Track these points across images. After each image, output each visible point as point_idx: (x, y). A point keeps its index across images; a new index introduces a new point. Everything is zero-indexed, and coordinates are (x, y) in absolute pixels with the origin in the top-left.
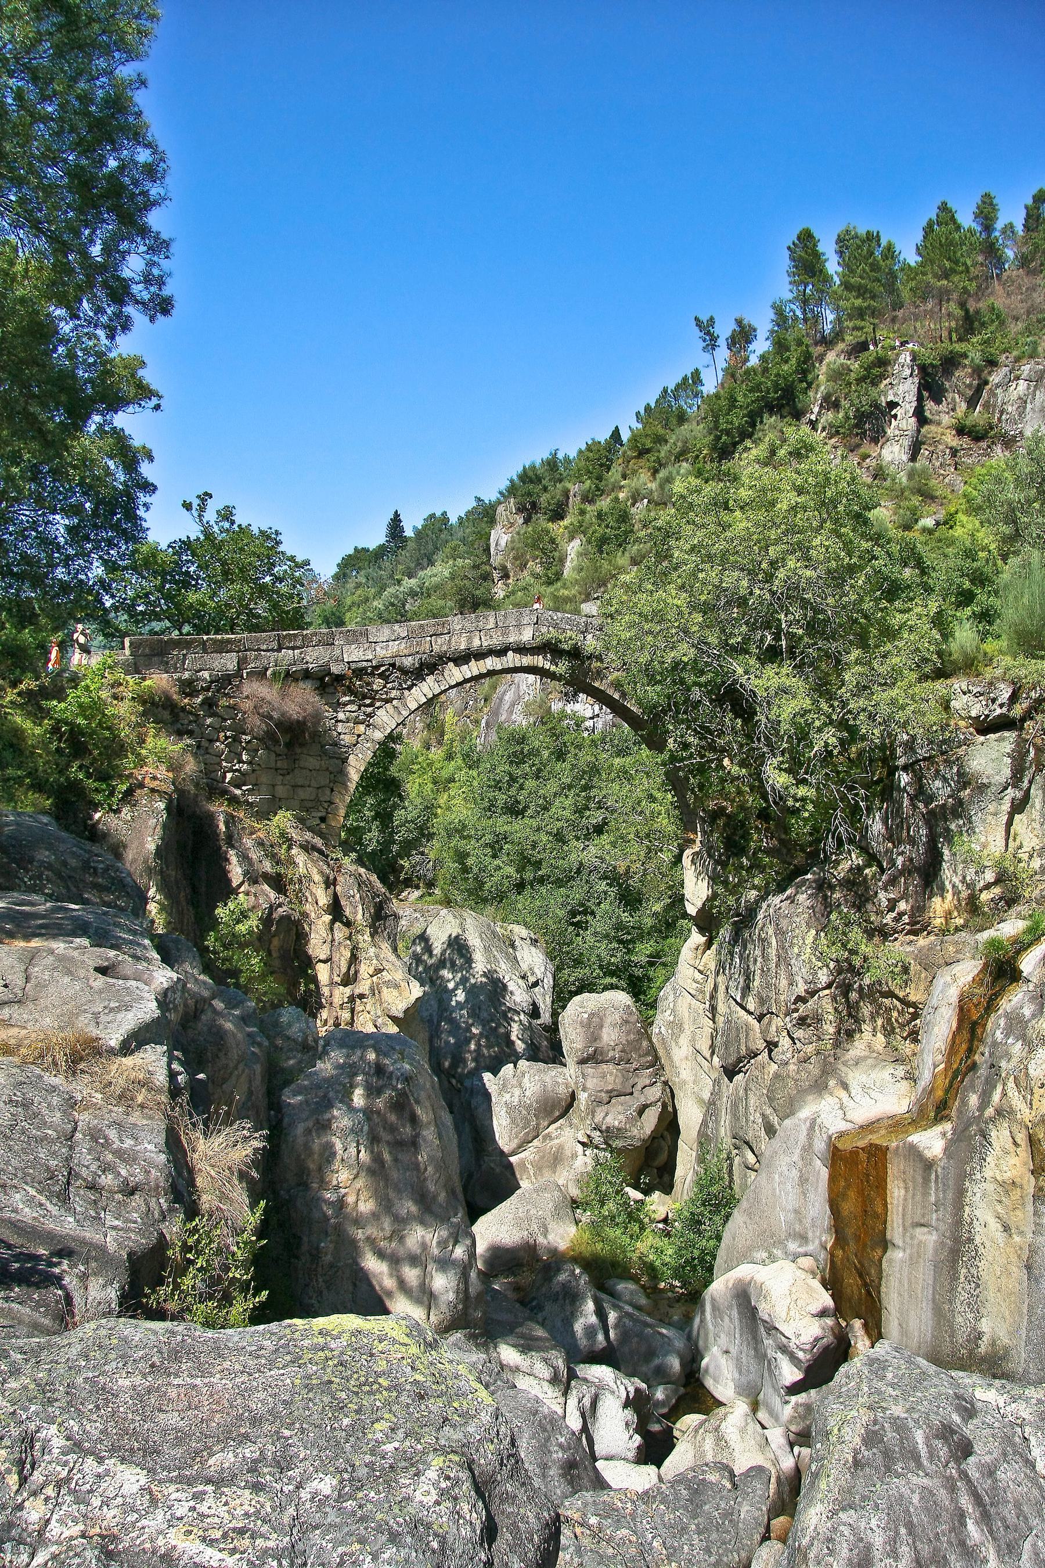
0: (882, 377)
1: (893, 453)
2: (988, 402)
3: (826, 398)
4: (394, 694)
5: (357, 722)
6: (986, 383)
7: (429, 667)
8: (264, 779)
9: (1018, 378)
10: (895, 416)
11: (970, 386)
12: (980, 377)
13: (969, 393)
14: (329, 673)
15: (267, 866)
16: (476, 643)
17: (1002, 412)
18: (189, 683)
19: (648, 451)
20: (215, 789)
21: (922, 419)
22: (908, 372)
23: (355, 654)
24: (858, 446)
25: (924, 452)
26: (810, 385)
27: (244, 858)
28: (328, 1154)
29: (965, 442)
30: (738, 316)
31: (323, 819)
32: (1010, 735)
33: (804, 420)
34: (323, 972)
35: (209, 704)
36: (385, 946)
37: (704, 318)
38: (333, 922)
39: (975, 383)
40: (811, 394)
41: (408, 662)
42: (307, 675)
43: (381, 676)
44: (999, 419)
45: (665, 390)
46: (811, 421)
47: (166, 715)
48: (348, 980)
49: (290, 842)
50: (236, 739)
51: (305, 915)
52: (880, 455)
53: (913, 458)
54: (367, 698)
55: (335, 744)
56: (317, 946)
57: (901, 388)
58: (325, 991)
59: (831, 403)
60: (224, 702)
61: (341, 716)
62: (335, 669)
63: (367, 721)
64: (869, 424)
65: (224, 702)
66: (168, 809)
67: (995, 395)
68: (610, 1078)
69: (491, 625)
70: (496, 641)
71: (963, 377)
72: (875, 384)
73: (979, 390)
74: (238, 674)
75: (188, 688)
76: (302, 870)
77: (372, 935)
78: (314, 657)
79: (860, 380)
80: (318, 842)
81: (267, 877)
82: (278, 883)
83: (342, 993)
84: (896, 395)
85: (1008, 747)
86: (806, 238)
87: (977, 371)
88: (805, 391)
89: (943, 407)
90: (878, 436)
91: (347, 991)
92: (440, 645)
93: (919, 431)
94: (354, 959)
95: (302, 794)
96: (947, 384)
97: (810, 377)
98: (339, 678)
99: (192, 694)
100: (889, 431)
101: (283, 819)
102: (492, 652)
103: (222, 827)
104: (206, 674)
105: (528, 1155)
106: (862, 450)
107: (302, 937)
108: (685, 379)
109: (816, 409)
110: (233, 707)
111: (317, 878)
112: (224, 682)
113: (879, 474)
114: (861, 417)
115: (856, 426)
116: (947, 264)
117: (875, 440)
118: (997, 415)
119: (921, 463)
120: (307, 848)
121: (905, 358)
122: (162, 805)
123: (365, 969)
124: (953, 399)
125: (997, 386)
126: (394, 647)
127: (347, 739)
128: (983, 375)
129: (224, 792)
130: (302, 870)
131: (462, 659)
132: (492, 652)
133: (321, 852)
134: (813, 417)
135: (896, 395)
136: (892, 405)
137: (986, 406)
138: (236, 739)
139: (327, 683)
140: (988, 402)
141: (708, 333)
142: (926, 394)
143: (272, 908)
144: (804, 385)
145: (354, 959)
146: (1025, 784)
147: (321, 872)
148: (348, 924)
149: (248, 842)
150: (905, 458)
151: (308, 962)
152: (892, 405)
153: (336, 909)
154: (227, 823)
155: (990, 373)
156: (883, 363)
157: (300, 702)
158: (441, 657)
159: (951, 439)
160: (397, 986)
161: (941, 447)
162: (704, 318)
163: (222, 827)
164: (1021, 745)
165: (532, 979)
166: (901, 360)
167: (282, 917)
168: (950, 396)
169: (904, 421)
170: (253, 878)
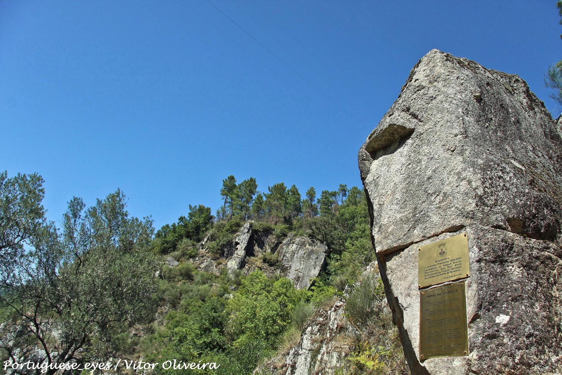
1: (232, 264)
2: (279, 251)
6: (281, 243)
9: (293, 243)
11: (273, 243)
12: (278, 240)
17: (284, 256)
21: (249, 251)
22: (246, 231)
24: (218, 258)
33: (200, 244)
39: (276, 242)
44: (282, 259)
46: (202, 245)
52: (226, 264)
57: (242, 237)
59: (213, 238)
67: (283, 248)
71: (272, 239)
73: (277, 245)
84: (239, 239)
87: (278, 237)
88: (203, 232)
93: (245, 257)
106: (219, 261)
109: (205, 240)
113: (224, 272)
116: (279, 196)
118: (282, 257)
119: (244, 271)
121: (247, 225)
134: (203, 243)
135: (239, 239)
137: (279, 253)
140: (279, 251)
144: (204, 229)
152: (237, 243)
155: (283, 240)
161: (254, 266)
166: (245, 226)
169: (240, 251)
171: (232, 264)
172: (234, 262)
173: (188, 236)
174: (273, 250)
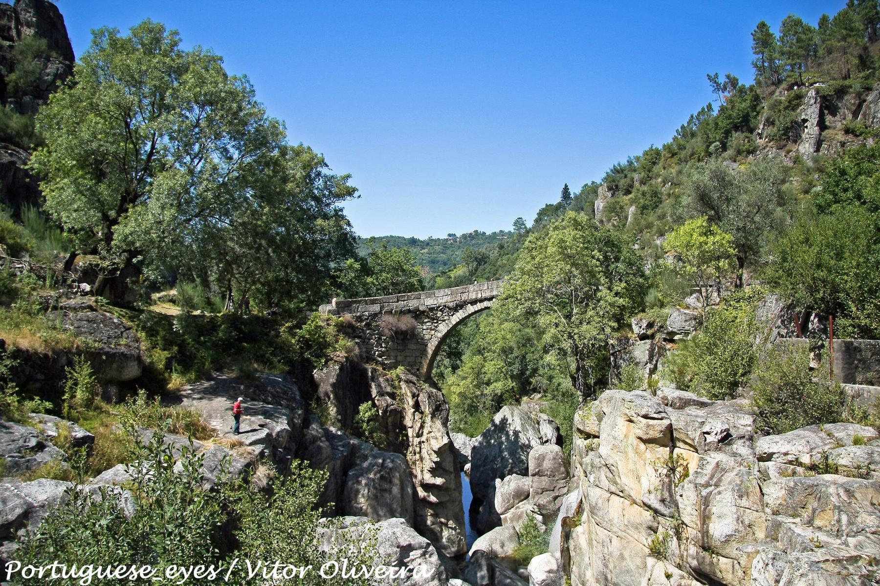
0: (798, 105)
1: (806, 148)
3: (767, 120)
4: (446, 318)
5: (431, 330)
6: (865, 101)
7: (460, 306)
8: (392, 354)
10: (806, 127)
11: (854, 104)
12: (860, 98)
13: (854, 108)
14: (419, 310)
15: (389, 389)
16: (479, 296)
17: (874, 118)
18: (360, 317)
19: (676, 154)
20: (370, 359)
21: (822, 126)
22: (813, 101)
23: (430, 302)
24: (785, 146)
25: (824, 146)
26: (758, 113)
27: (379, 386)
28: (357, 492)
29: (850, 137)
30: (727, 73)
31: (418, 370)
32: (648, 341)
33: (755, 133)
34: (410, 432)
35: (368, 325)
36: (438, 423)
37: (712, 75)
38: (414, 412)
39: (857, 102)
40: (759, 118)
41: (451, 305)
42: (409, 311)
43: (441, 310)
44: (872, 122)
45: (692, 116)
46: (759, 134)
47: (350, 330)
48: (419, 435)
49: (400, 380)
50: (380, 338)
51: (404, 409)
53: (817, 150)
54: (435, 320)
55: (422, 339)
56: (408, 422)
57: (809, 111)
58: (411, 439)
59: (770, 122)
60: (374, 324)
61: (425, 327)
62: (421, 308)
63: (435, 329)
64: (792, 133)
65: (374, 324)
66: (340, 369)
67: (870, 108)
68: (544, 483)
69: (486, 287)
70: (487, 294)
71: (850, 99)
72: (793, 109)
73: (860, 106)
74: (380, 312)
75: (359, 319)
76: (403, 391)
77: (432, 418)
78: (413, 304)
79: (786, 108)
80: (414, 379)
81: (388, 394)
82: (393, 396)
83: (417, 440)
84: (806, 115)
85: (648, 347)
86: (762, 26)
87: (859, 95)
88: (755, 117)
89: (838, 118)
90: (797, 139)
91: (418, 440)
92: (465, 297)
93: (820, 134)
94: (422, 427)
95: (409, 359)
96: (840, 105)
97: (758, 109)
98: (423, 312)
99: (361, 321)
100: (803, 136)
101: (400, 370)
102: (486, 299)
103: (370, 374)
104: (367, 313)
105: (509, 515)
106: (787, 148)
107: (403, 417)
108: (703, 109)
109: (761, 127)
110: (378, 326)
111: (409, 394)
112: (374, 316)
113: (797, 160)
114: (786, 130)
115: (784, 134)
116: (844, 32)
117: (795, 142)
118: (871, 120)
119: (823, 151)
120: (408, 382)
121: (812, 93)
122: (337, 367)
123: (425, 431)
124: (844, 113)
125: (871, 103)
126: (445, 299)
127: (427, 337)
128: (862, 97)
129: (375, 359)
130: (403, 391)
131: (474, 302)
132: (486, 299)
133: (414, 384)
134: (760, 131)
135: (806, 115)
136: (805, 121)
137: (864, 115)
138: (380, 338)
139: (418, 314)
141: (715, 82)
142: (826, 112)
143: (387, 406)
144: (755, 113)
145: (422, 427)
146: (654, 362)
147: (411, 392)
148: (422, 413)
149: (381, 379)
150: (812, 150)
151: (405, 428)
152: (805, 121)
153: (417, 406)
154: (372, 373)
155: (867, 95)
156: (799, 97)
157: (406, 322)
158: (465, 302)
159: (841, 137)
160: (436, 438)
162: (712, 75)
163: (370, 374)
164: (652, 345)
165: (545, 439)
166: (809, 94)
167: (392, 410)
168: (841, 111)
169: (811, 130)
170: (381, 394)
171: (806, 148)
172: (807, 145)
173: (736, 128)
174: (855, 114)
